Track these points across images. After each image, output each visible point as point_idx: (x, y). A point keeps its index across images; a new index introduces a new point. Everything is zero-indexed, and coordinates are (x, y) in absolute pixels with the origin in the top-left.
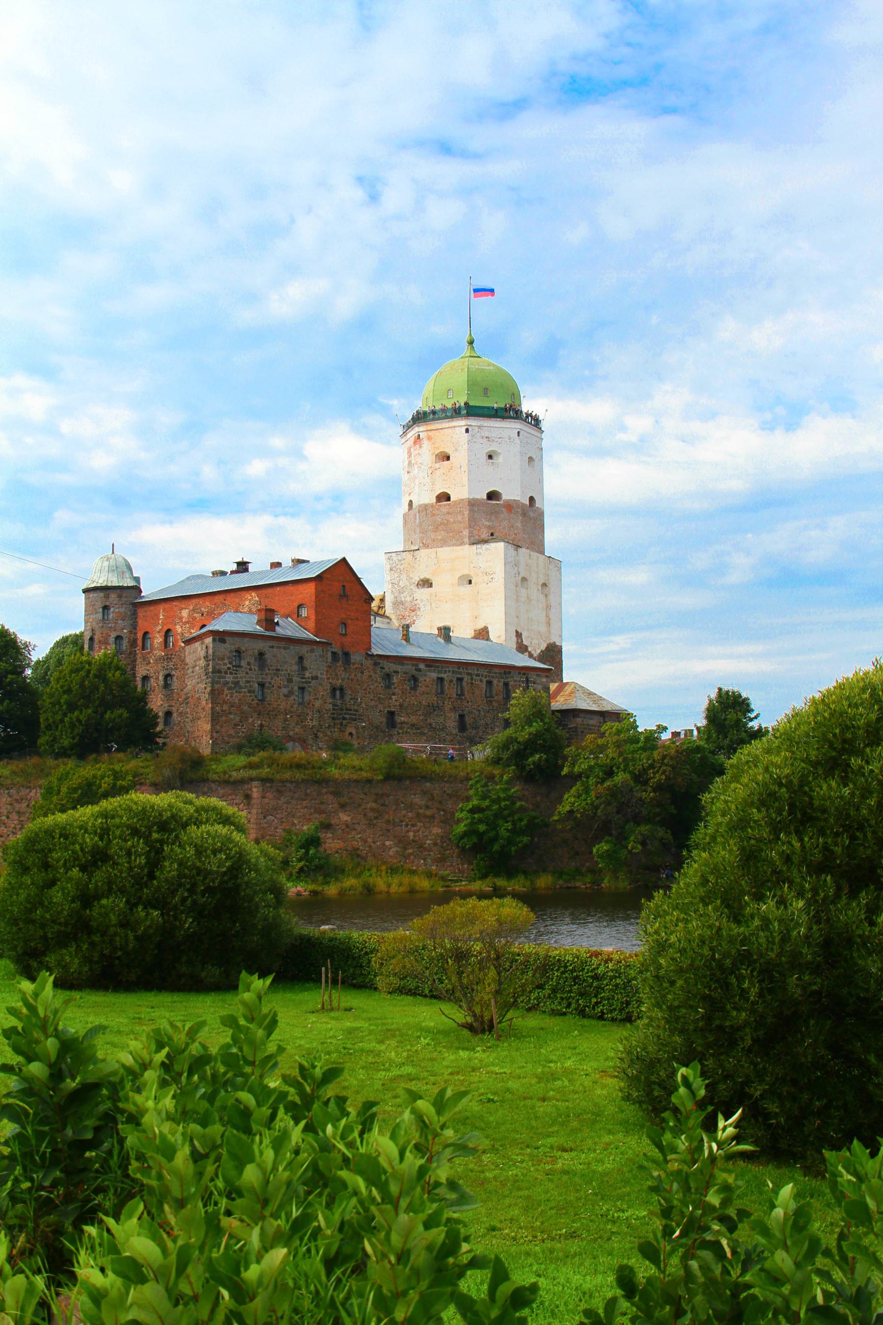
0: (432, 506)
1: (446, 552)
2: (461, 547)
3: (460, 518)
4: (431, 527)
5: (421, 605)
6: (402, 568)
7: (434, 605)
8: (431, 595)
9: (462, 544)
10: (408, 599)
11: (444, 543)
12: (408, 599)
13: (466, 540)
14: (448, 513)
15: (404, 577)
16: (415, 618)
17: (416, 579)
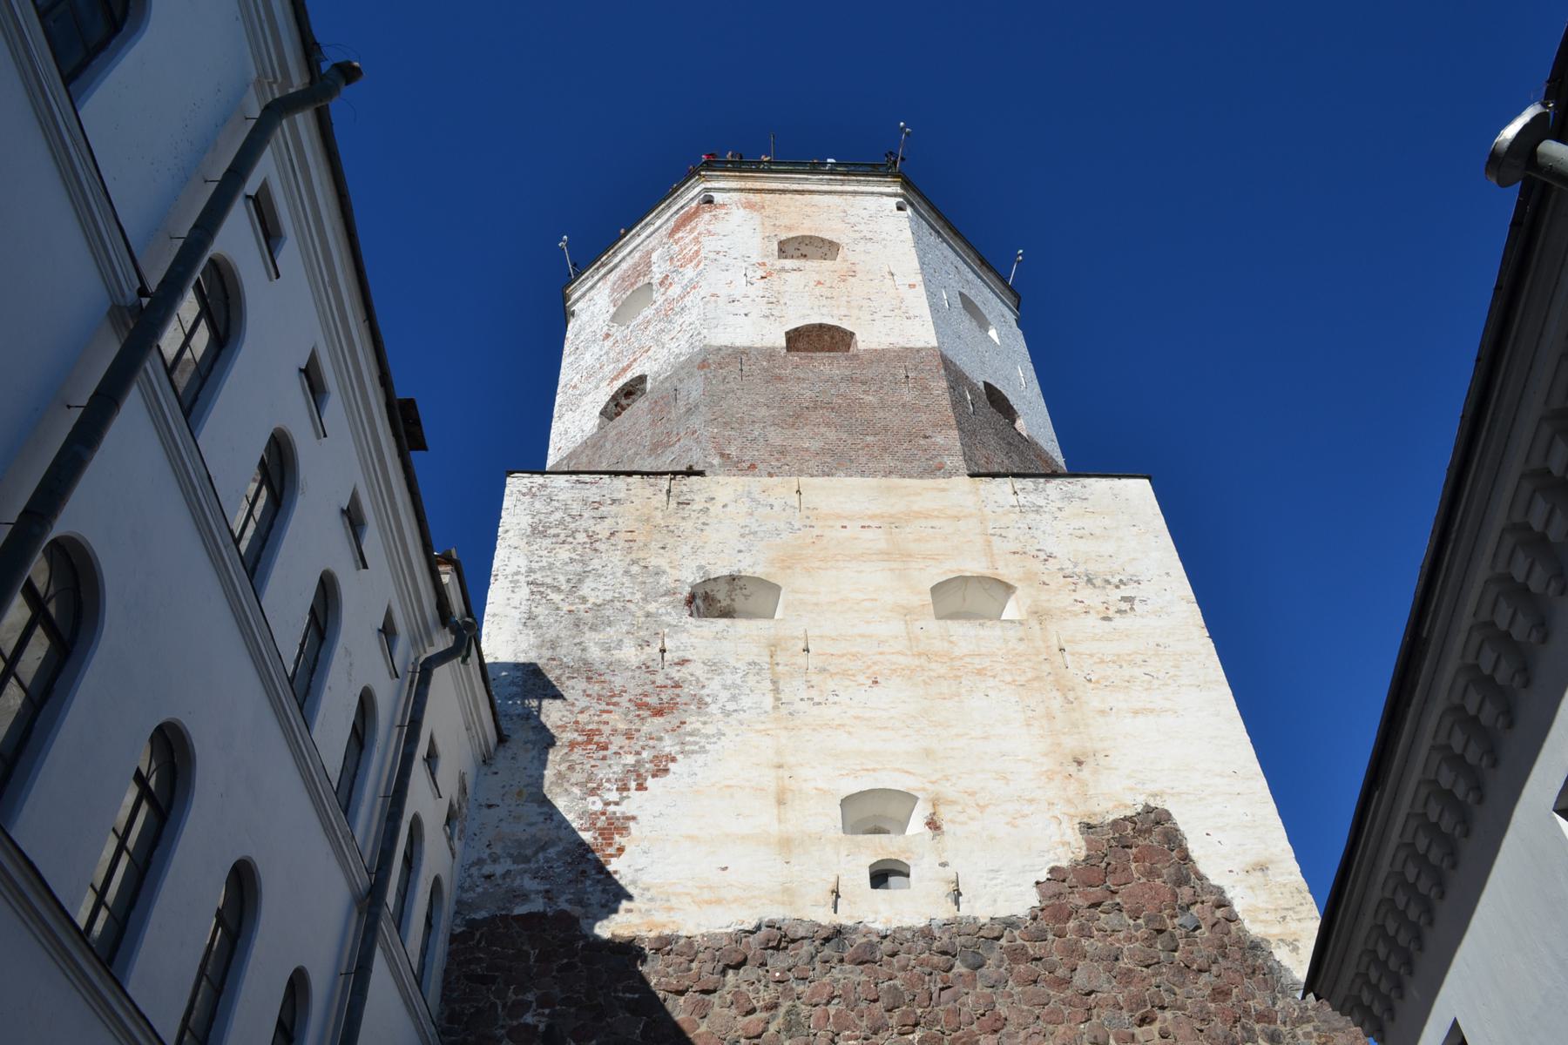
0: (770, 354)
1: (847, 496)
2: (928, 483)
3: (908, 395)
4: (763, 412)
5: (714, 686)
6: (602, 529)
7: (793, 690)
8: (774, 647)
9: (934, 470)
10: (630, 654)
11: (835, 462)
12: (630, 654)
13: (955, 461)
14: (852, 380)
15: (612, 560)
16: (668, 746)
17: (688, 576)
